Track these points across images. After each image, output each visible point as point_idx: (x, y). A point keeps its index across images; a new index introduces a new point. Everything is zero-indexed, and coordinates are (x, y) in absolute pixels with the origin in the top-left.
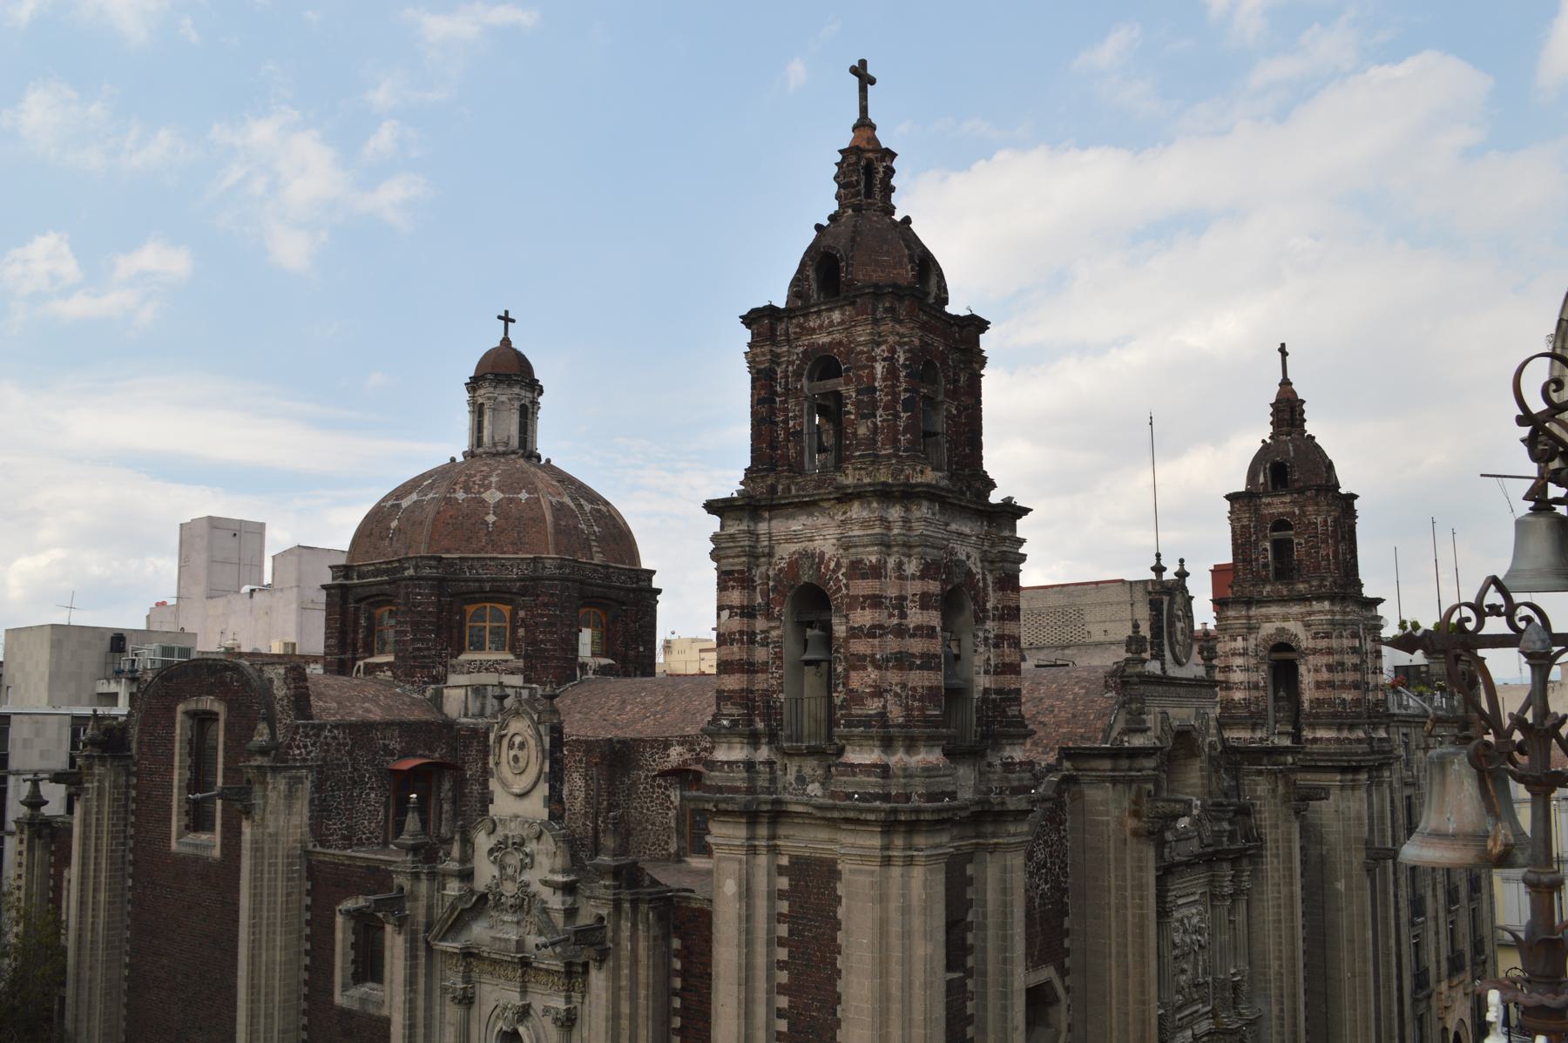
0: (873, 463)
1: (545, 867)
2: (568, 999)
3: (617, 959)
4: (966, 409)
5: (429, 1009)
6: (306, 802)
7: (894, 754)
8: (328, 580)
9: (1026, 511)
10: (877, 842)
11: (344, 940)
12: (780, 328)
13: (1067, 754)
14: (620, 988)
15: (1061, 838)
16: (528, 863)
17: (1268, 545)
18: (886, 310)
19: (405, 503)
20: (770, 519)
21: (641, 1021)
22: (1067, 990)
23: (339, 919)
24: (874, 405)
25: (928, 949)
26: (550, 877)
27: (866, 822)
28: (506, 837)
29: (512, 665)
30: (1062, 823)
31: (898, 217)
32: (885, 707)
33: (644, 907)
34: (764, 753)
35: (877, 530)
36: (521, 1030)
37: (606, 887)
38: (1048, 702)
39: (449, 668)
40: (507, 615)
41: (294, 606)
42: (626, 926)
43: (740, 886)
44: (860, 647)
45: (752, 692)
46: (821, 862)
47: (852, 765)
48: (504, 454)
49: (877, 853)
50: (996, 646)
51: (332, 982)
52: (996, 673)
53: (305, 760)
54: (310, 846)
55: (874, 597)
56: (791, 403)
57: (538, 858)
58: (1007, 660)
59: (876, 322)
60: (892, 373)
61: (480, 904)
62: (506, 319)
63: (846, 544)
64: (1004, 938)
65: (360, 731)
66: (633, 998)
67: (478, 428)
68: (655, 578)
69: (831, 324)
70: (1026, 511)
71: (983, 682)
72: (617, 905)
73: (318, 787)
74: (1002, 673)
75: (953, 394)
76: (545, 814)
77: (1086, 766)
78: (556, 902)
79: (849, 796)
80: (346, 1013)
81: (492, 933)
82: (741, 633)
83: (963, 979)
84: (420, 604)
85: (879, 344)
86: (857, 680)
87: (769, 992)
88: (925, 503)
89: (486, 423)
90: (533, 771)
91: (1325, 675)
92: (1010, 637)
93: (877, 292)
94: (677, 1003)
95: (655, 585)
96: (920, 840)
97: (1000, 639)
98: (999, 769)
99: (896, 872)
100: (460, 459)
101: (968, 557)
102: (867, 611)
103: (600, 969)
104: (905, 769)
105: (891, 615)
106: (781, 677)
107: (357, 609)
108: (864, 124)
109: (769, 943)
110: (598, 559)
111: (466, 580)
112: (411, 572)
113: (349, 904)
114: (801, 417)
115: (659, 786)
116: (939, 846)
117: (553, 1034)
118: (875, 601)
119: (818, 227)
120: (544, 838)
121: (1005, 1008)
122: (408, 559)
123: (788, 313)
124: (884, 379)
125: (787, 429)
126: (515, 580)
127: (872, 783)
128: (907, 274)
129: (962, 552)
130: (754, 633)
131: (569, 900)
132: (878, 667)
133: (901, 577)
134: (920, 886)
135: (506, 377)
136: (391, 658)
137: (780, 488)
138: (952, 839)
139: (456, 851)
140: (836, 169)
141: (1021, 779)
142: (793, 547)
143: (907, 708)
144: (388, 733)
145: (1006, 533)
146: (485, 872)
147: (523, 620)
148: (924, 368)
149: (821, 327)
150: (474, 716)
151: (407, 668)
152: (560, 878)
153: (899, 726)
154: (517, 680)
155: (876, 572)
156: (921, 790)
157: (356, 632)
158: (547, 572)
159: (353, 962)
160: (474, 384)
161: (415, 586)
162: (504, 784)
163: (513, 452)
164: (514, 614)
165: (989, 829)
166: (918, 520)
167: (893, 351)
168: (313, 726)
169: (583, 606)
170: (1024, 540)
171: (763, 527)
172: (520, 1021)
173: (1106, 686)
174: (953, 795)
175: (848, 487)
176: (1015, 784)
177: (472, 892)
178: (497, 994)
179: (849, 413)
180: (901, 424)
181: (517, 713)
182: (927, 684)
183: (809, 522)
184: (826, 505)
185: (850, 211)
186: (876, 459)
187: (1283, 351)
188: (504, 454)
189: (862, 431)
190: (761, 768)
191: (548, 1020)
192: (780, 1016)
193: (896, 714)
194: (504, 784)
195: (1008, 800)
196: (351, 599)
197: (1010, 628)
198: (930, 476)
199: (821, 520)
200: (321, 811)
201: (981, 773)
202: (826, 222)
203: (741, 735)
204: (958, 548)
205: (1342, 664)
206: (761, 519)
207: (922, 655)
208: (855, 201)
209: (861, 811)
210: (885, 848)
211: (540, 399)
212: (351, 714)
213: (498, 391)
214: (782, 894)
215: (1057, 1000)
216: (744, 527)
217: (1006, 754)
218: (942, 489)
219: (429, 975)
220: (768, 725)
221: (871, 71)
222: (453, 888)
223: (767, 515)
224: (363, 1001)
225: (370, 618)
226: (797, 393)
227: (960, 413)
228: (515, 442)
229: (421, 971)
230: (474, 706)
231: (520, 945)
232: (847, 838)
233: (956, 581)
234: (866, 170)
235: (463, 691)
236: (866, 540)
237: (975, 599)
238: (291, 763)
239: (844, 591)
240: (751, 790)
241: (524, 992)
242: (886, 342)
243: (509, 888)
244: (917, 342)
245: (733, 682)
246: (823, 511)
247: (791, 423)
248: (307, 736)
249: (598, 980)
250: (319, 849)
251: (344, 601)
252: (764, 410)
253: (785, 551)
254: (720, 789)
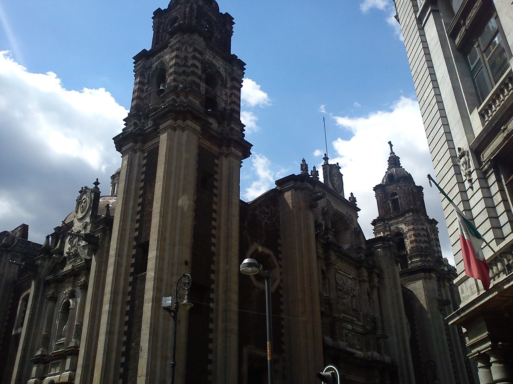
17: (389, 202)
22: (280, 266)
36: (71, 301)
50: (230, 97)
91: (413, 238)
187: (390, 143)
205: (419, 234)
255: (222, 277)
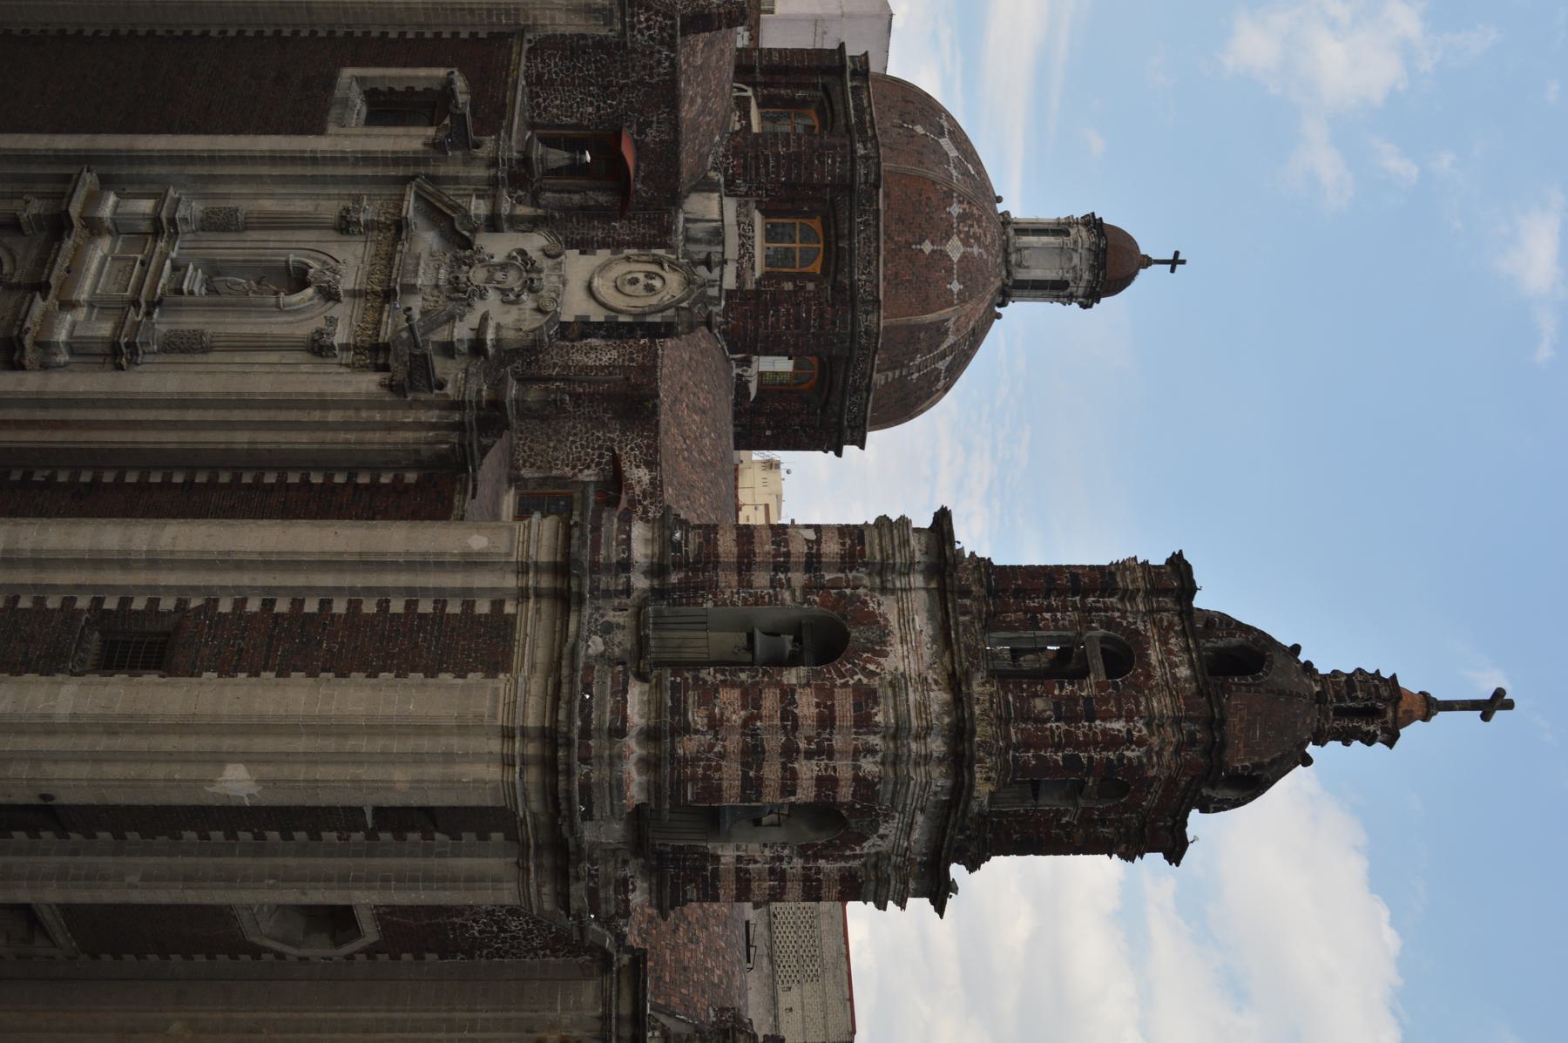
0: (999, 717)
1: (505, 319)
2: (345, 347)
3: (393, 406)
4: (1068, 835)
5: (335, 180)
6: (582, 30)
7: (639, 743)
8: (851, 51)
9: (940, 910)
10: (532, 721)
11: (418, 78)
12: (1167, 602)
13: (639, 959)
14: (358, 409)
15: (534, 950)
16: (509, 298)
18: (1192, 734)
19: (945, 142)
20: (927, 590)
21: (318, 436)
22: (350, 957)
23: (441, 72)
24: (1072, 719)
25: (401, 784)
26: (492, 324)
27: (555, 709)
28: (540, 271)
29: (748, 275)
30: (554, 952)
31: (1311, 749)
32: (697, 732)
33: (454, 437)
34: (640, 582)
35: (915, 723)
36: (310, 291)
37: (479, 391)
38: (703, 935)
39: (743, 199)
40: (809, 269)
41: (818, 11)
42: (432, 416)
43: (479, 554)
44: (770, 702)
45: (715, 568)
46: (508, 654)
47: (625, 691)
48: (1007, 262)
49: (518, 723)
50: (772, 871)
51: (367, 66)
52: (738, 870)
53: (633, 28)
54: (529, 36)
55: (833, 719)
56: (1073, 616)
57: (514, 309)
58: (754, 885)
59: (1177, 721)
60: (1113, 741)
61: (459, 241)
62: (1175, 262)
63: (897, 684)
64: (414, 879)
65: (669, 95)
66: (345, 426)
67: (1038, 230)
68: (855, 448)
69: (1173, 665)
70: (940, 910)
71: (727, 854)
72: (458, 405)
73: (600, 44)
74: (739, 879)
75: (1086, 820)
76: (567, 317)
77: (624, 982)
78: (462, 331)
79: (587, 688)
80: (330, 82)
81: (425, 256)
82: (788, 554)
83: (364, 827)
84: (822, 163)
85: (1148, 725)
86: (729, 698)
87: (352, 590)
88: (948, 783)
89: (1045, 239)
90: (619, 302)
92: (783, 888)
93: (1215, 723)
94: (339, 479)
95: (847, 449)
96: (533, 775)
97: (780, 876)
98: (620, 873)
99: (495, 745)
100: (1000, 208)
101: (882, 837)
102: (814, 711)
103: (381, 385)
104: (621, 757)
105: (809, 740)
106: (733, 604)
107: (815, 86)
108: (1429, 707)
109: (409, 590)
110: (878, 379)
111: (851, 219)
112: (861, 152)
113: (460, 84)
114: (1056, 628)
115: (601, 456)
116: (526, 800)
117: (304, 330)
118: (826, 720)
119: (1296, 649)
120: (539, 316)
121: (329, 879)
122: (877, 147)
123: (1187, 612)
124: (1104, 732)
125: (1040, 610)
126: (851, 277)
127: (603, 716)
128: (1239, 760)
129: (889, 828)
130: (787, 570)
131: (464, 348)
132: (746, 722)
133: (856, 754)
134: (479, 774)
135: (1102, 262)
136: (756, 128)
137: (967, 602)
138: (534, 815)
139: (522, 210)
140: (1371, 670)
141: (607, 901)
142: (893, 618)
143: (695, 760)
144: (665, 127)
145: (912, 885)
146: (497, 246)
147: (803, 288)
148: (1120, 782)
149: (1170, 652)
150: (686, 230)
151: (744, 149)
152: (490, 336)
153: (673, 749)
154: (730, 282)
155: (863, 722)
156: (594, 777)
157: (787, 86)
158: (862, 317)
159: (391, 90)
160: (1093, 223)
161: (843, 157)
162: (604, 268)
163: (1009, 273)
164: (810, 277)
165: (547, 861)
166: (928, 774)
167: (1141, 742)
168: (673, 37)
169: (820, 359)
170: (903, 907)
171: (918, 580)
172: (320, 290)
173: (723, 1010)
174: (588, 816)
175: (969, 686)
176: (602, 895)
177: (474, 231)
178: (352, 262)
179: (1062, 688)
180: (1048, 753)
181: (689, 282)
182: (725, 784)
183: (925, 638)
184: (946, 659)
185: (1317, 689)
186: (1004, 721)
188: (1007, 262)
189: (1039, 704)
190: (622, 580)
191: (320, 323)
192: (322, 602)
193: (688, 746)
194: (604, 268)
195: (582, 884)
196: (827, 79)
197: (794, 888)
198: (983, 789)
199: (927, 652)
200: (570, 47)
201: (614, 851)
202: (1302, 658)
203: (662, 554)
204: (894, 824)
206: (928, 579)
207: (760, 779)
208: (1331, 695)
209: (570, 702)
210: (524, 732)
211: (1075, 305)
212: (688, 82)
213: (1084, 253)
214: (469, 605)
215: (338, 945)
216: (918, 557)
217: (638, 883)
218: (967, 804)
219: (375, 180)
220: (674, 588)
221: (1499, 715)
222: (479, 208)
223: (933, 585)
224: (346, 103)
225: (804, 103)
226: (1086, 623)
227: (1060, 826)
228: (1022, 275)
229: (380, 171)
230: (697, 229)
231: (411, 289)
232: (536, 685)
233: (853, 821)
234: (1370, 709)
235: (716, 216)
236: (903, 709)
237: (830, 844)
238: (629, 10)
239: (839, 682)
240: (595, 568)
241: (354, 294)
242: (1152, 734)
243: (478, 275)
244: (1152, 773)
245: (727, 544)
246: (938, 655)
247: (1047, 615)
248: (662, 29)
249: (368, 383)
250: (526, 46)
251: (827, 71)
252: (1064, 581)
253: (888, 608)
254: (596, 529)
255: (107, 862)
